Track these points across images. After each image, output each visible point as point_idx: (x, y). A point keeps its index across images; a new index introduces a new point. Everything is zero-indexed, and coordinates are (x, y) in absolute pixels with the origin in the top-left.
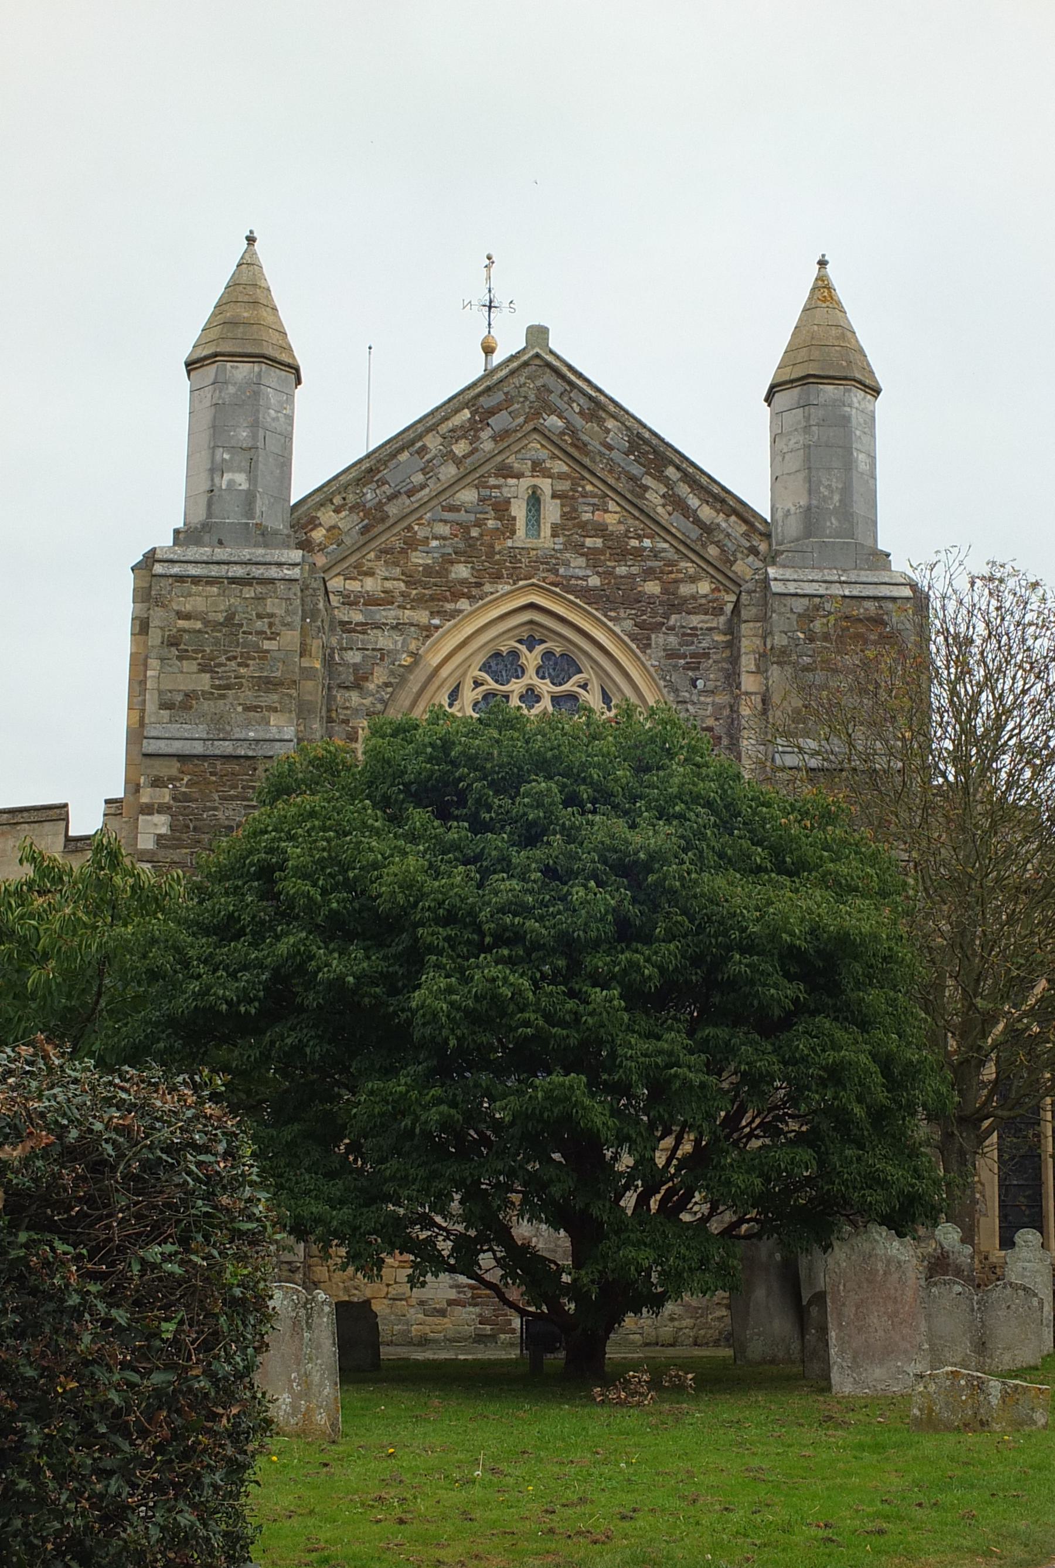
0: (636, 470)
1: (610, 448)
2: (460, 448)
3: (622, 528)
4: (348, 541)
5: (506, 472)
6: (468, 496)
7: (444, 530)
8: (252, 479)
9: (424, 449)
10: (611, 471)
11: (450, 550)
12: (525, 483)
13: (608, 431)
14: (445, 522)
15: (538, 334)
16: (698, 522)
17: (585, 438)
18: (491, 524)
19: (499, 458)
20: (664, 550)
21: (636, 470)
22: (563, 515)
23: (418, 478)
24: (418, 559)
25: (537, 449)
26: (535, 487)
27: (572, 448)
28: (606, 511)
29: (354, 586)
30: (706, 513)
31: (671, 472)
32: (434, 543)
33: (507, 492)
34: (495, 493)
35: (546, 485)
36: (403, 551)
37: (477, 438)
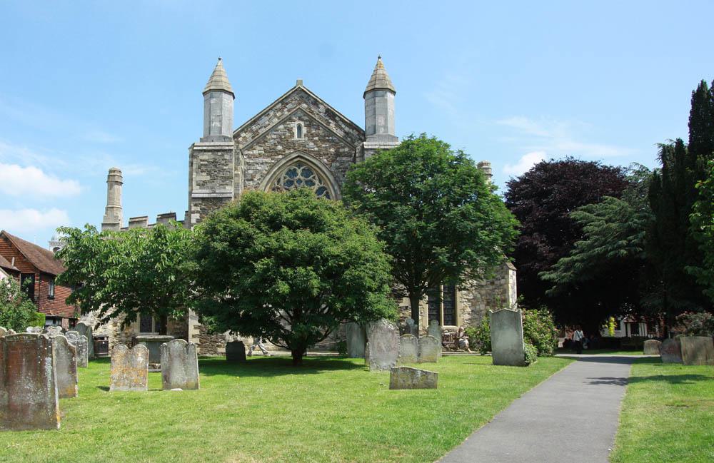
2: (278, 114)
12: (297, 123)
18: (288, 134)
22: (307, 132)
23: (267, 123)
31: (337, 118)
33: (292, 126)
37: (283, 111)
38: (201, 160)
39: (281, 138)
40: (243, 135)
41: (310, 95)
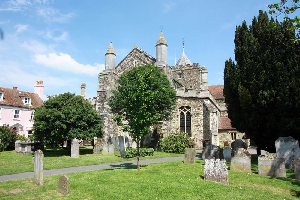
0: (145, 57)
2: (129, 59)
8: (109, 65)
12: (135, 61)
33: (133, 62)
38: (101, 79)
39: (130, 67)
40: (118, 67)
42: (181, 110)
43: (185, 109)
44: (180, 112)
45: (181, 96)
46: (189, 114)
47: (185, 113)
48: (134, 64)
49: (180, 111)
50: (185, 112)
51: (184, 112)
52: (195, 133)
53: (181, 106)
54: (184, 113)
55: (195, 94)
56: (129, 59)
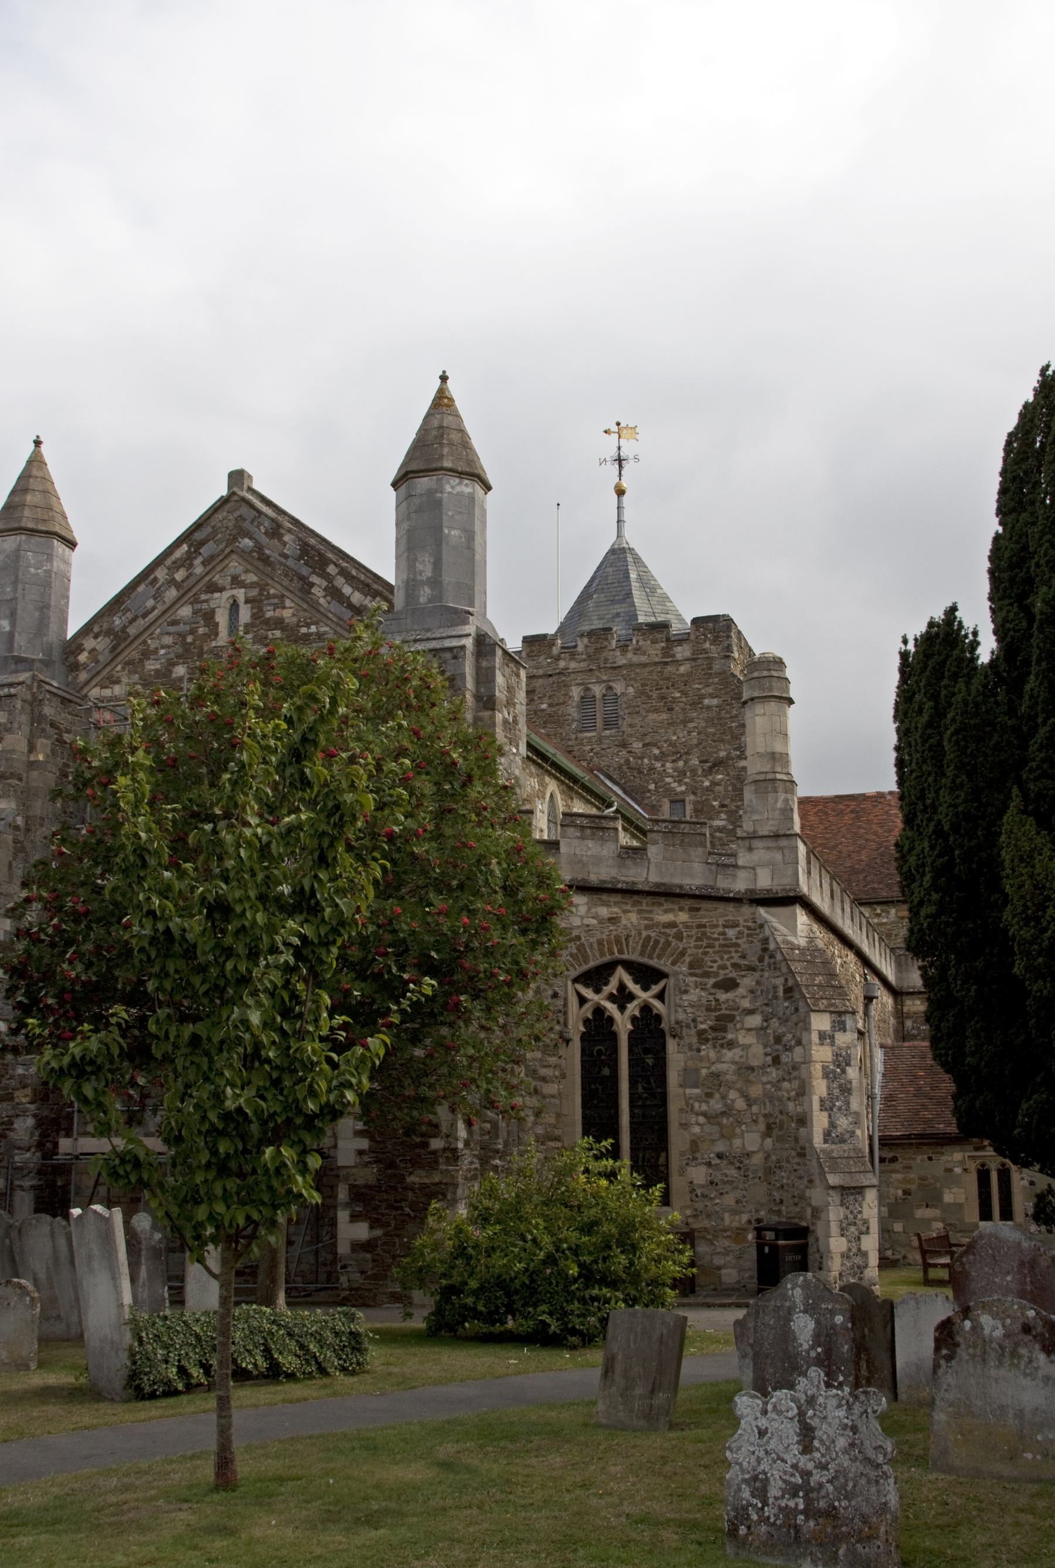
0: (305, 571)
1: (286, 557)
2: (179, 576)
3: (295, 619)
4: (101, 658)
5: (214, 588)
6: (186, 611)
7: (168, 640)
8: (13, 624)
9: (156, 579)
10: (286, 575)
11: (172, 656)
12: (226, 595)
13: (285, 544)
14: (168, 634)
15: (237, 477)
16: (350, 606)
17: (267, 552)
18: (201, 631)
19: (207, 579)
20: (326, 633)
21: (305, 571)
22: (253, 615)
23: (150, 603)
24: (151, 666)
25: (235, 566)
26: (233, 596)
27: (260, 559)
28: (284, 608)
29: (107, 692)
30: (357, 598)
31: (331, 569)
32: (162, 652)
33: (212, 604)
34: (205, 606)
35: (240, 594)
36: (141, 661)
37: (191, 565)
39: (184, 644)
40: (89, 643)
41: (260, 512)
42: (588, 993)
43: (622, 987)
44: (587, 1011)
45: (594, 878)
46: (648, 1026)
47: (623, 1024)
48: (222, 618)
49: (582, 1000)
50: (622, 1008)
51: (611, 1008)
52: (699, 1174)
53: (592, 964)
54: (611, 1020)
55: (698, 867)
56: (179, 576)
